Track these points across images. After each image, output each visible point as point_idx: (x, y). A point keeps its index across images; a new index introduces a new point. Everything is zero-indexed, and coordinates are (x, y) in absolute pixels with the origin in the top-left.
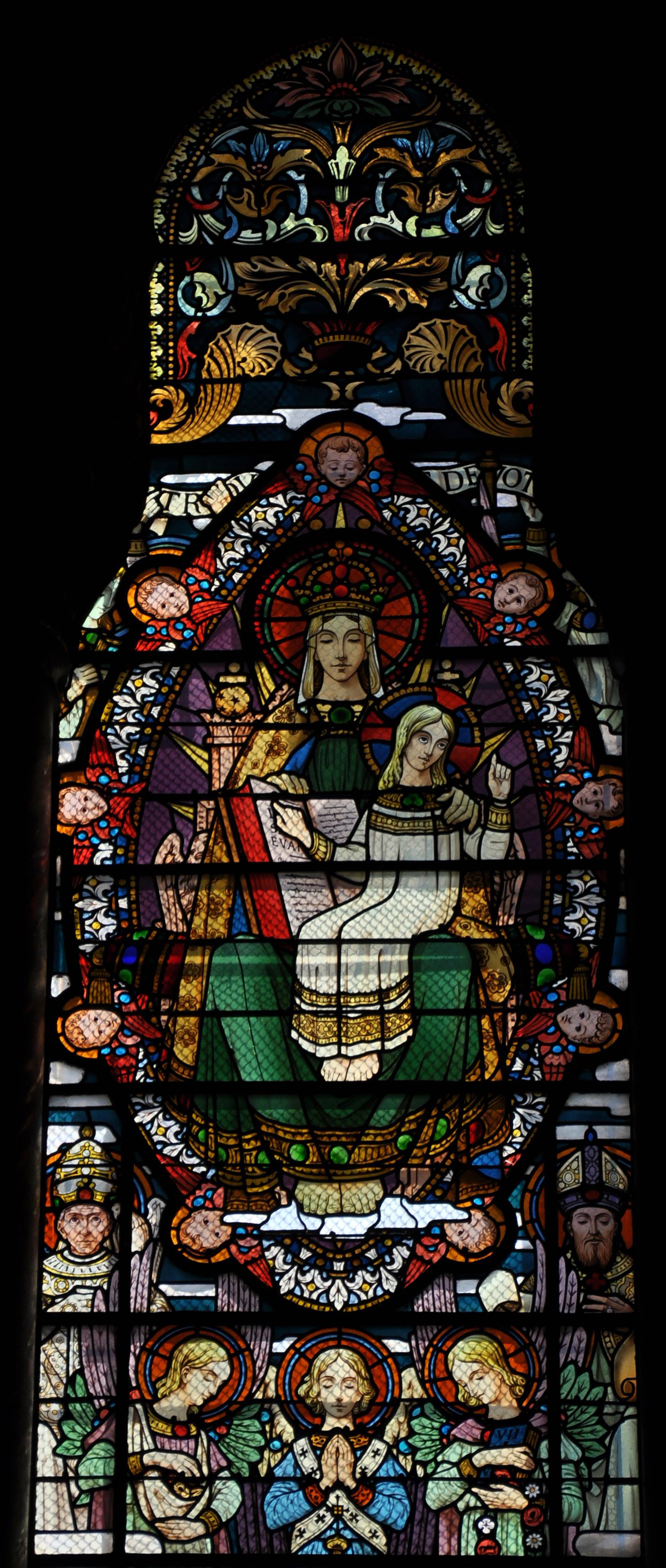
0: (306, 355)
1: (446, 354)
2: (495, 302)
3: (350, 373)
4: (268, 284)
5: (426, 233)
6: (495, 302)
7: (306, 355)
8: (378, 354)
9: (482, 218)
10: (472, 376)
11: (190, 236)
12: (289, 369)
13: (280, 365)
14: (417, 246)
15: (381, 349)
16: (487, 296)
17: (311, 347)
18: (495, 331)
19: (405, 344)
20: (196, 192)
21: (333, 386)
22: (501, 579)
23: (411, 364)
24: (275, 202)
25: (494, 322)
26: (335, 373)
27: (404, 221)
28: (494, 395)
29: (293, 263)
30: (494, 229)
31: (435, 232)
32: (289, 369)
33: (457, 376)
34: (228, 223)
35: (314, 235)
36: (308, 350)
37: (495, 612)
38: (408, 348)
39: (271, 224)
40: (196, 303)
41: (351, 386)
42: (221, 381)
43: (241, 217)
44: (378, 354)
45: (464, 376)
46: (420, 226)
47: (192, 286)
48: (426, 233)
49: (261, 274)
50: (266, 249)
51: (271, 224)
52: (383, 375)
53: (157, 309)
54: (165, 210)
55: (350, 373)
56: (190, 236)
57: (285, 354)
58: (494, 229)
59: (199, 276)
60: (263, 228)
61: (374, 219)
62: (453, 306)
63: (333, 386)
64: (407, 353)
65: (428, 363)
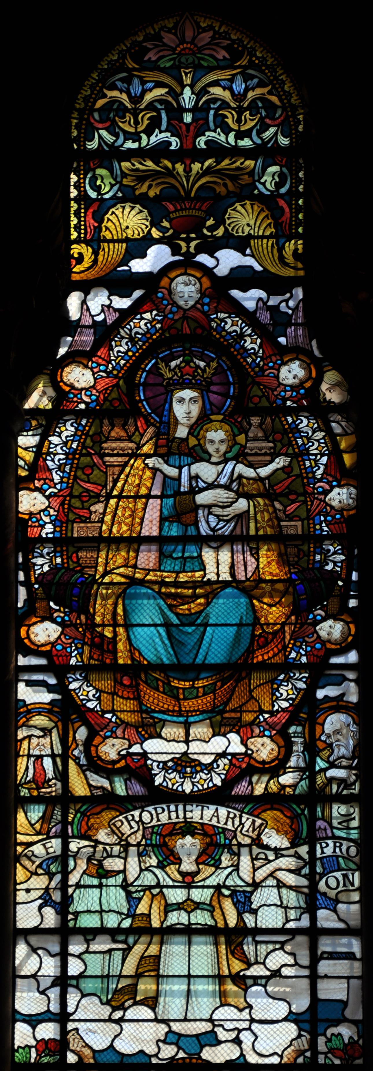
0: (166, 224)
1: (252, 223)
2: (283, 191)
3: (193, 235)
4: (141, 177)
5: (241, 143)
6: (283, 191)
7: (166, 224)
8: (210, 222)
9: (276, 134)
10: (268, 238)
11: (93, 145)
12: (155, 233)
13: (149, 232)
14: (236, 152)
15: (212, 219)
16: (279, 185)
17: (168, 218)
18: (282, 209)
19: (227, 216)
21: (183, 244)
22: (284, 364)
23: (230, 229)
24: (146, 122)
25: (282, 203)
26: (184, 236)
27: (227, 135)
28: (281, 249)
29: (157, 164)
30: (284, 141)
31: (246, 143)
32: (155, 233)
33: (258, 237)
34: (117, 136)
35: (170, 144)
36: (167, 221)
37: (280, 384)
38: (229, 218)
39: (144, 136)
40: (97, 189)
41: (193, 244)
42: (113, 241)
43: (125, 132)
44: (210, 222)
45: (263, 237)
46: (237, 137)
47: (94, 179)
48: (241, 143)
49: (137, 170)
50: (141, 153)
51: (144, 136)
52: (212, 236)
53: (74, 193)
54: (78, 127)
55: (193, 235)
56: (93, 145)
57: (153, 224)
58: (284, 141)
59: (100, 171)
60: (139, 140)
61: (207, 133)
62: (256, 192)
63: (183, 244)
64: (228, 222)
65: (241, 229)
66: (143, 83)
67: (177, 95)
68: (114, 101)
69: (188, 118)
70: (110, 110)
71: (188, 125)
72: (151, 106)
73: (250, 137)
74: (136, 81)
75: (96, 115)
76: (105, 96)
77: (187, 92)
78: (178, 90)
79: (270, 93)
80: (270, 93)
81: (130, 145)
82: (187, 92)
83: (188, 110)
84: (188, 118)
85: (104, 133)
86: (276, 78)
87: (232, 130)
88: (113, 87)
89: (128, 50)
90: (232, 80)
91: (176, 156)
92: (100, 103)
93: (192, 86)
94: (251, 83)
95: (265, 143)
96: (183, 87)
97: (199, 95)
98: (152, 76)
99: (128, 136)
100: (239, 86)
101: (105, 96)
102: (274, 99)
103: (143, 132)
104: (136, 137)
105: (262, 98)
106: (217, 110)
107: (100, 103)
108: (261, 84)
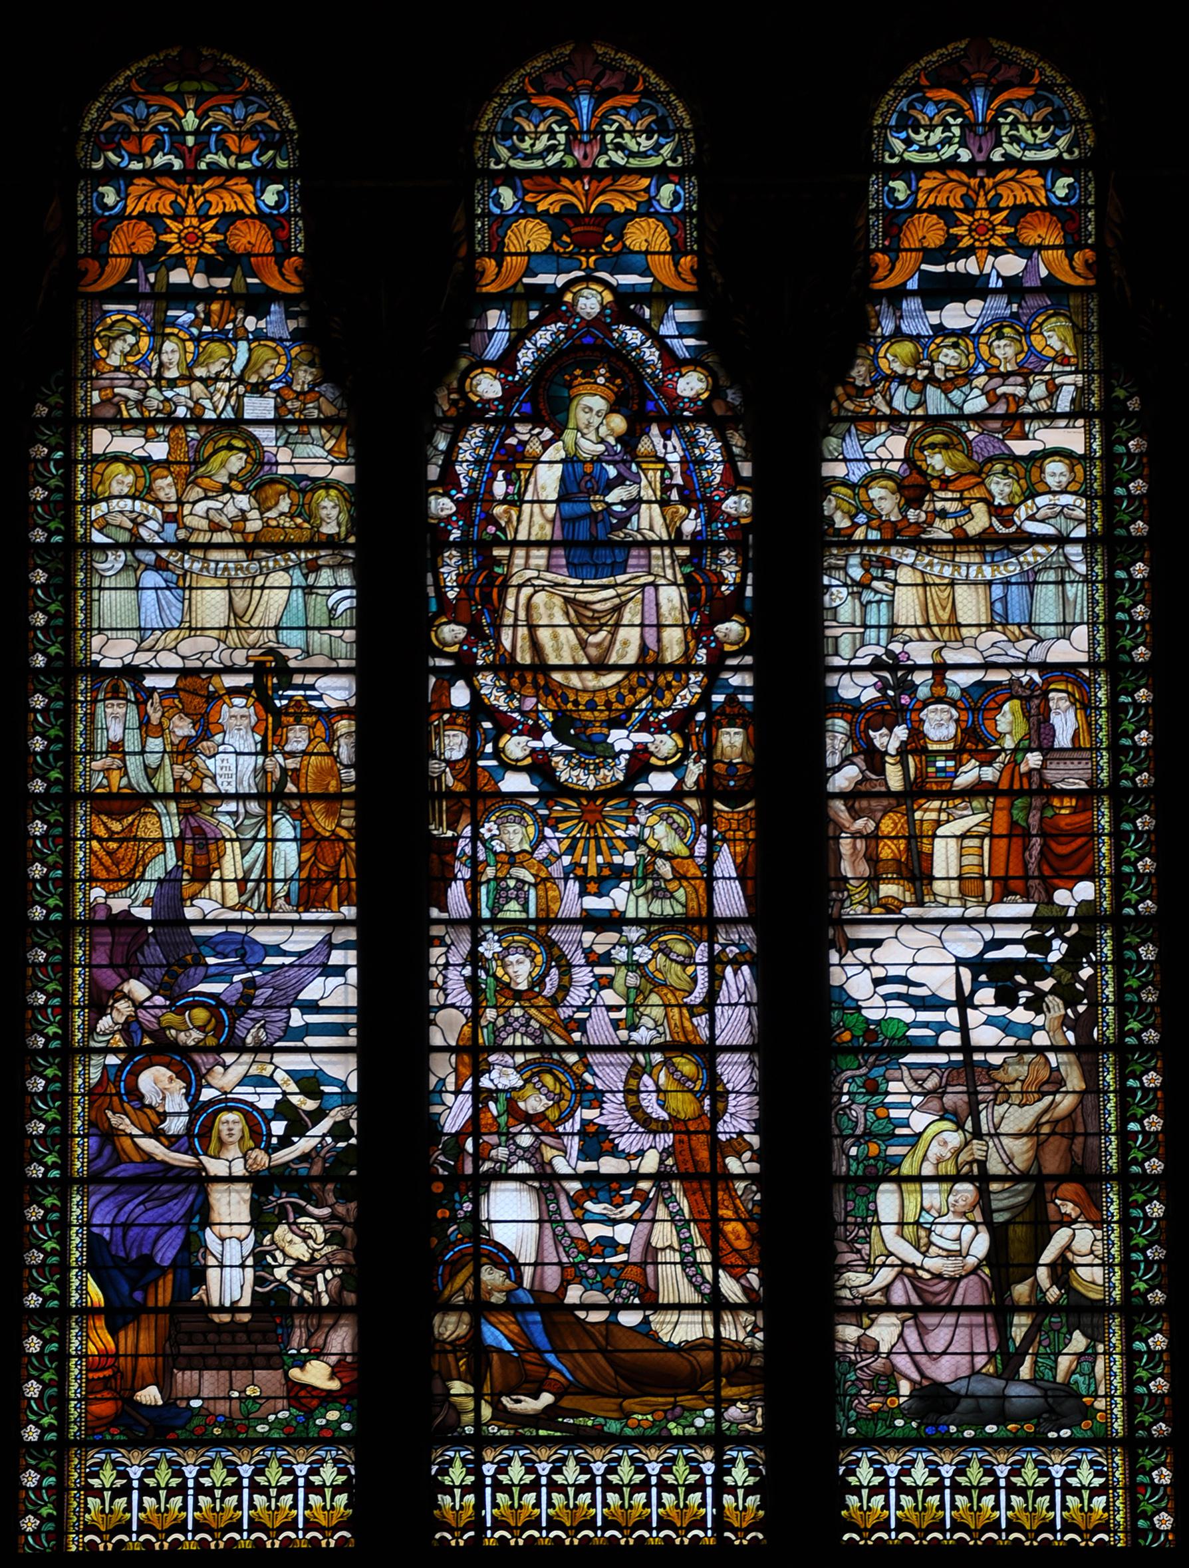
11: (98, 165)
20: (102, 138)
34: (122, 157)
56: (98, 165)
60: (144, 161)
66: (148, 107)
67: (179, 119)
68: (119, 123)
69: (190, 141)
70: (116, 133)
71: (190, 149)
72: (154, 130)
73: (250, 160)
74: (141, 104)
75: (102, 138)
76: (110, 118)
77: (191, 114)
78: (182, 113)
79: (270, 118)
80: (270, 118)
81: (136, 166)
82: (191, 114)
83: (190, 133)
84: (190, 141)
85: (110, 155)
86: (275, 104)
87: (232, 153)
88: (119, 110)
89: (135, 75)
90: (232, 106)
91: (178, 176)
92: (107, 125)
93: (195, 110)
94: (252, 108)
95: (264, 166)
96: (186, 111)
97: (202, 117)
98: (155, 100)
99: (132, 157)
100: (239, 112)
101: (110, 118)
102: (273, 124)
103: (148, 154)
104: (140, 158)
105: (261, 123)
106: (219, 133)
107: (107, 125)
108: (261, 109)
